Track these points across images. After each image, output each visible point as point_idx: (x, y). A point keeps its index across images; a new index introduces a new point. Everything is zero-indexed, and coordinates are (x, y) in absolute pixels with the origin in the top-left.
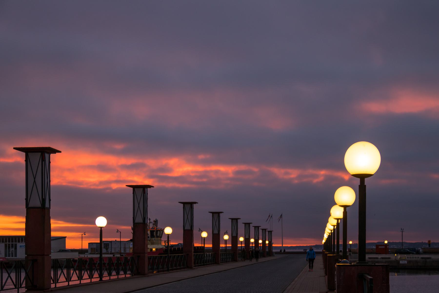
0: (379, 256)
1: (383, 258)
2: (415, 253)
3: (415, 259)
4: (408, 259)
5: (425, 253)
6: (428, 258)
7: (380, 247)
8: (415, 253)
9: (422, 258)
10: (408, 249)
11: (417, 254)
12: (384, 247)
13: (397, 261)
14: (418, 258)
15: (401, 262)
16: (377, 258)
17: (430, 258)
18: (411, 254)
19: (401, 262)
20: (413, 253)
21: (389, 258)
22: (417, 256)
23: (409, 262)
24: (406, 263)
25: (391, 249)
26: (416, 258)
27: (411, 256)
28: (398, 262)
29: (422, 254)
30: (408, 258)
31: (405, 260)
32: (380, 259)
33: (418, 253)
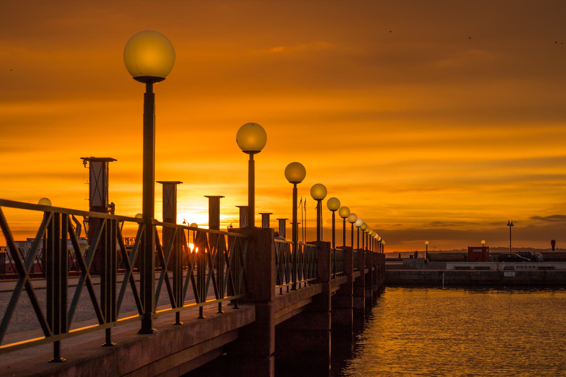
0: (472, 265)
1: (477, 268)
2: (529, 260)
3: (528, 269)
4: (518, 269)
5: (546, 260)
6: (549, 268)
7: (475, 250)
8: (529, 260)
9: (541, 268)
10: (519, 253)
11: (532, 262)
12: (481, 251)
13: (499, 272)
14: (534, 267)
15: (506, 274)
16: (469, 268)
17: (553, 268)
18: (523, 262)
19: (506, 274)
20: (526, 261)
21: (488, 268)
22: (532, 264)
23: (519, 274)
24: (514, 276)
25: (493, 254)
26: (530, 267)
27: (523, 264)
28: (501, 274)
29: (541, 261)
30: (517, 267)
31: (512, 269)
32: (474, 269)
33: (534, 259)
